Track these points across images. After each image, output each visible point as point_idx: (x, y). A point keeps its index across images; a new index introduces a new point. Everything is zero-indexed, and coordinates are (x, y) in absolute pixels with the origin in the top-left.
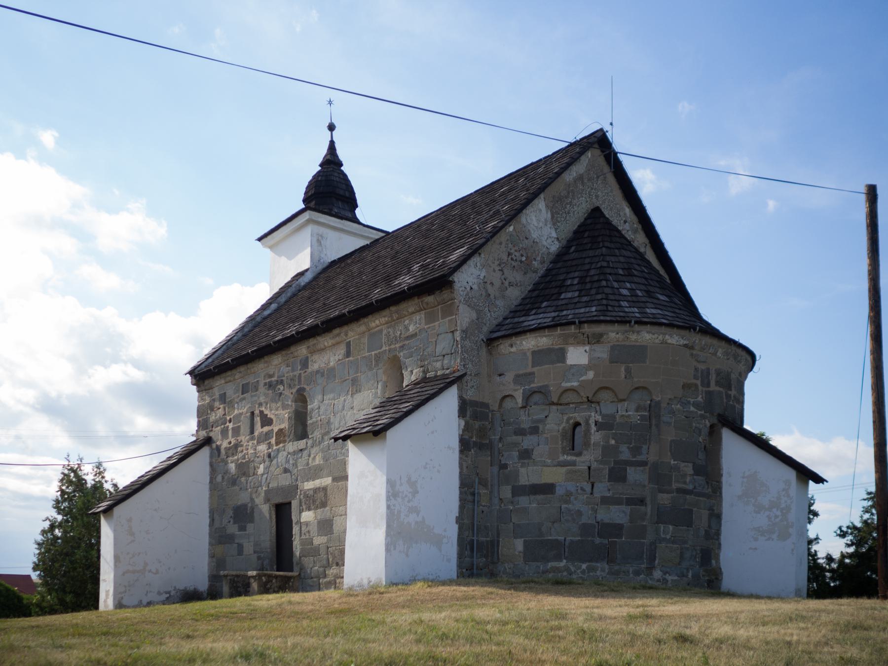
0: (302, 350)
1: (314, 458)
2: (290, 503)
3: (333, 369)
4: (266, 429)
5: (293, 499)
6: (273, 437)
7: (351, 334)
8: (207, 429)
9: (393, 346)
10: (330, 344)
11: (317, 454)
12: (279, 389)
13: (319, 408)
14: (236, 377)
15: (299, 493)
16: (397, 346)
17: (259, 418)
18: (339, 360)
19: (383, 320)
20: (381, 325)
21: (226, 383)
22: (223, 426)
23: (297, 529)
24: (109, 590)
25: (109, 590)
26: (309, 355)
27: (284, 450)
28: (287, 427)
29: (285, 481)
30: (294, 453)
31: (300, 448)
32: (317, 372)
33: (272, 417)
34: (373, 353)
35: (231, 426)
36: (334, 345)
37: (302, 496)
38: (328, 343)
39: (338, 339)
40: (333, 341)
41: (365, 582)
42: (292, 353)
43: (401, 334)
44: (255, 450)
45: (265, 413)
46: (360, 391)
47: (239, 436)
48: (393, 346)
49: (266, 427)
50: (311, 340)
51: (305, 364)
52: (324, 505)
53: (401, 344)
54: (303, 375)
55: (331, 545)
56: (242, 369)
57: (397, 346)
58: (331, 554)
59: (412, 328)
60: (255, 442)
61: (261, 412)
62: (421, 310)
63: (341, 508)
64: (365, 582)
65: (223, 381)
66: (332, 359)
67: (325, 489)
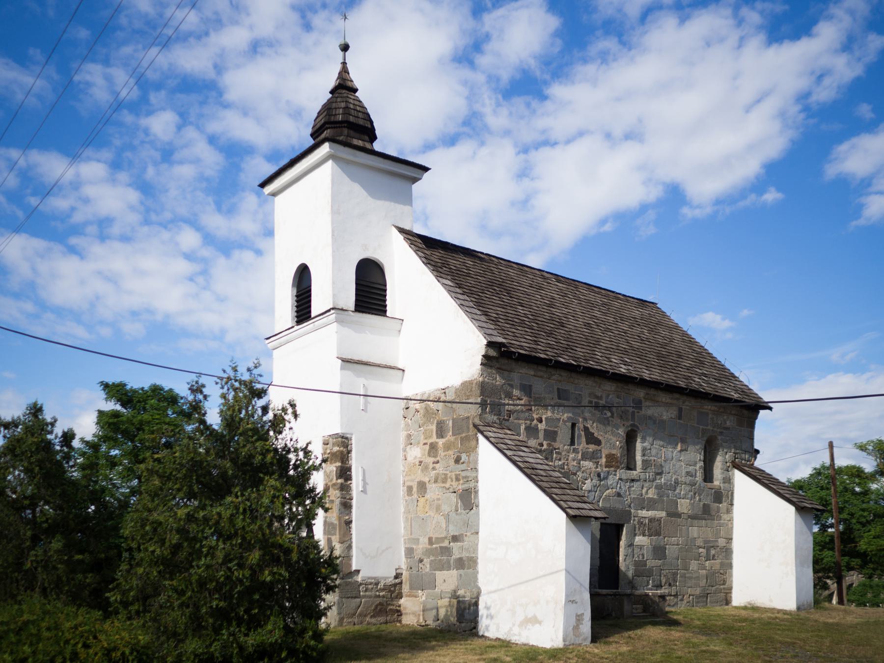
0: (640, 393)
1: (647, 493)
2: (622, 526)
3: (663, 422)
4: (592, 447)
5: (628, 523)
6: (601, 458)
7: (687, 403)
8: (500, 415)
9: (715, 429)
10: (667, 401)
11: (650, 488)
12: (605, 414)
13: (650, 449)
14: (554, 377)
15: (633, 518)
16: (719, 430)
17: (583, 433)
18: (671, 418)
19: (713, 408)
20: (710, 410)
21: (534, 376)
22: (528, 422)
23: (630, 550)
24: (583, 614)
25: (583, 614)
26: (643, 400)
27: (615, 475)
28: (619, 455)
29: (617, 505)
30: (627, 481)
31: (633, 477)
32: (650, 418)
33: (600, 438)
34: (701, 427)
35: (542, 426)
36: (667, 403)
37: (636, 523)
38: (666, 400)
39: (675, 402)
40: (668, 400)
41: (805, 603)
42: (629, 390)
43: (721, 423)
44: (579, 463)
45: (591, 430)
46: (687, 451)
47: (555, 442)
48: (715, 429)
49: (593, 445)
50: (652, 389)
51: (638, 404)
52: (658, 534)
53: (721, 431)
54: (636, 414)
55: (665, 568)
56: (565, 374)
57: (719, 430)
58: (665, 576)
59: (728, 424)
60: (580, 457)
61: (586, 429)
62: (737, 415)
63: (673, 538)
64: (805, 603)
65: (532, 373)
66: (665, 413)
67: (659, 520)
